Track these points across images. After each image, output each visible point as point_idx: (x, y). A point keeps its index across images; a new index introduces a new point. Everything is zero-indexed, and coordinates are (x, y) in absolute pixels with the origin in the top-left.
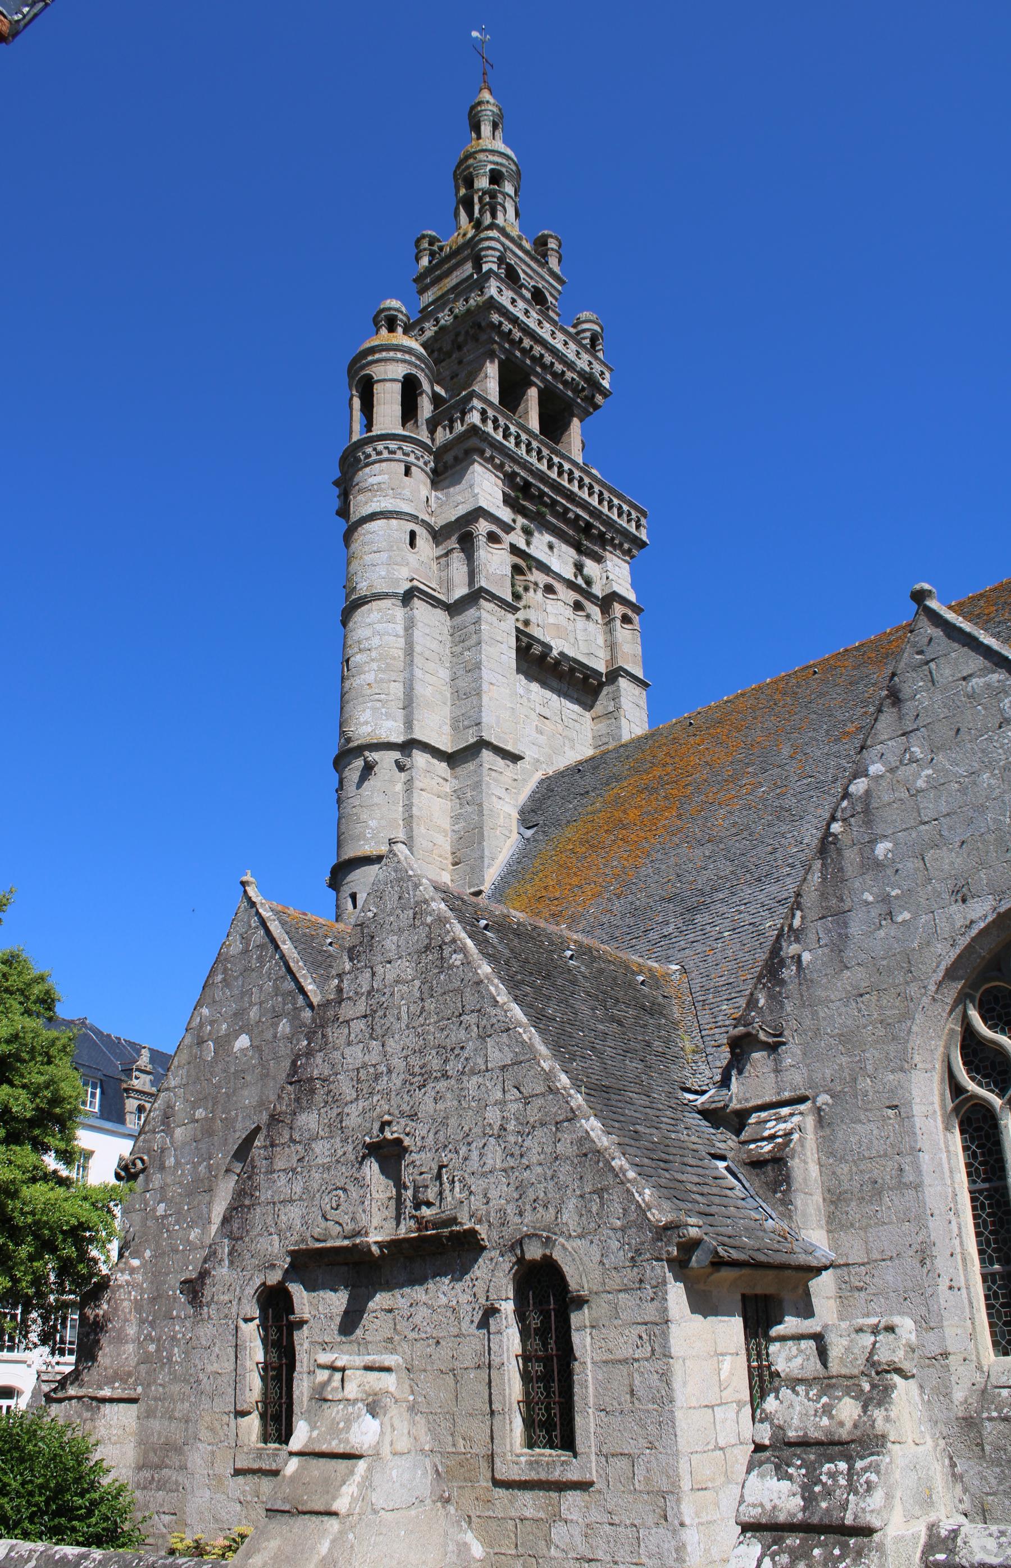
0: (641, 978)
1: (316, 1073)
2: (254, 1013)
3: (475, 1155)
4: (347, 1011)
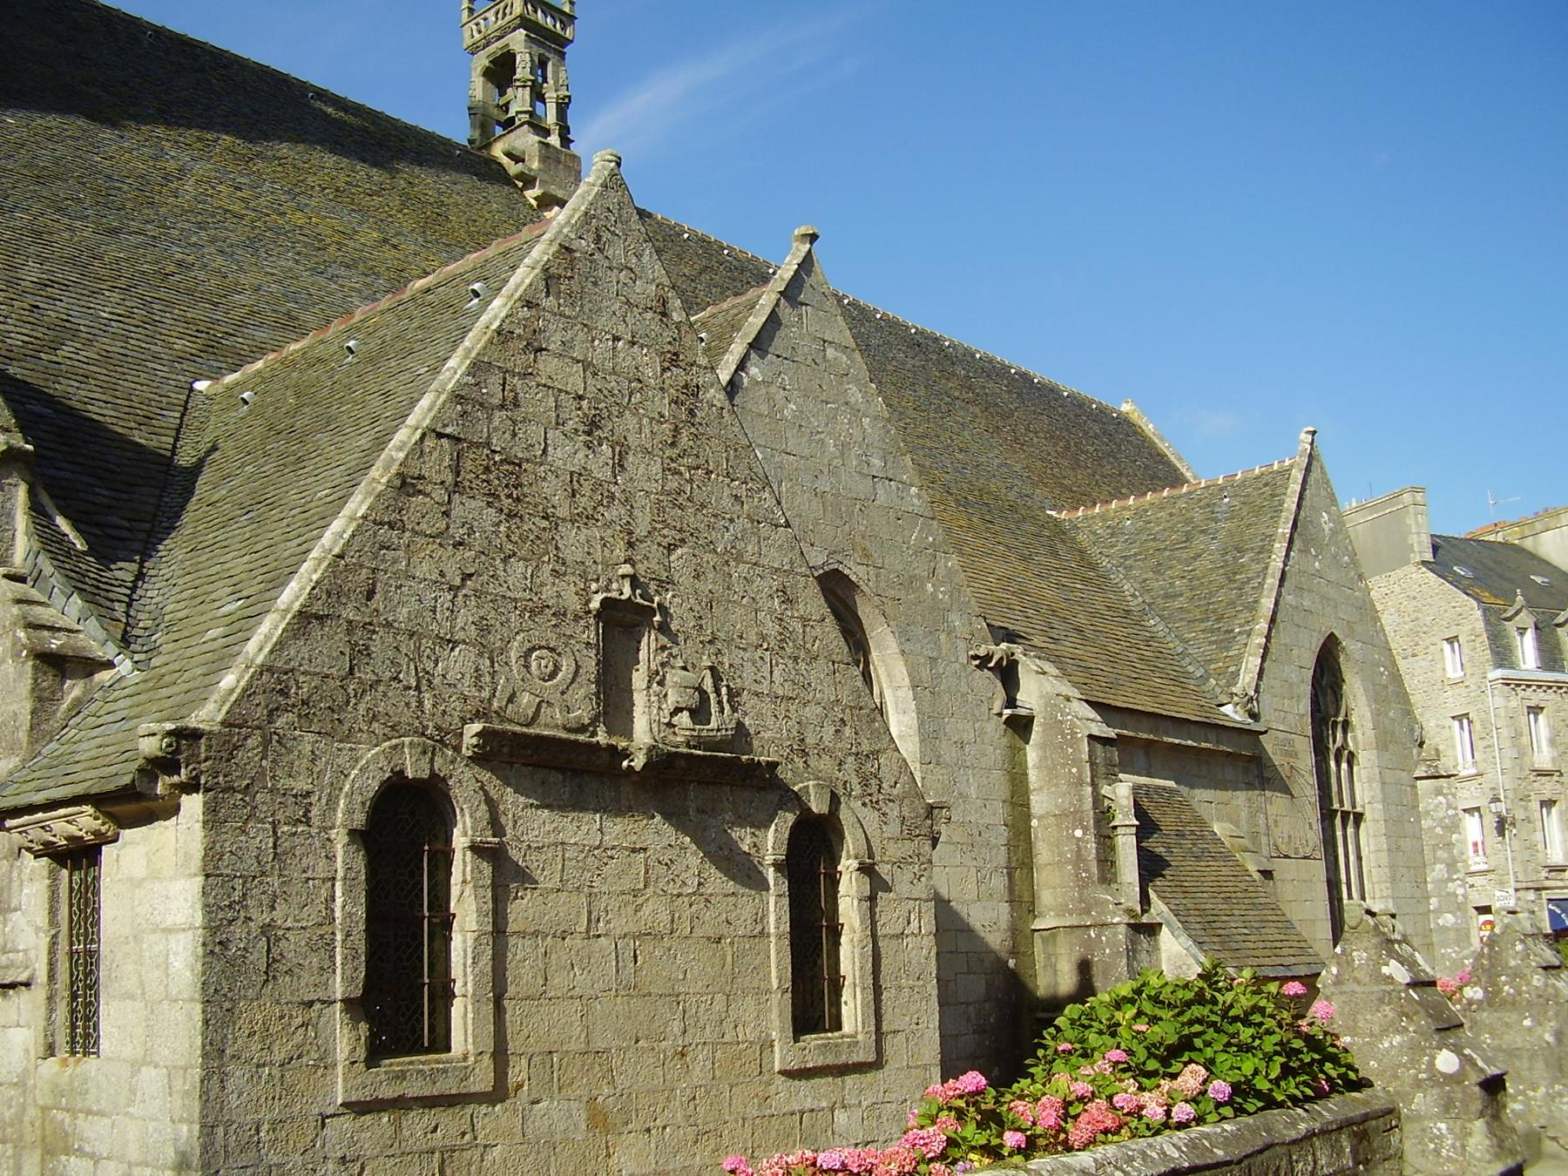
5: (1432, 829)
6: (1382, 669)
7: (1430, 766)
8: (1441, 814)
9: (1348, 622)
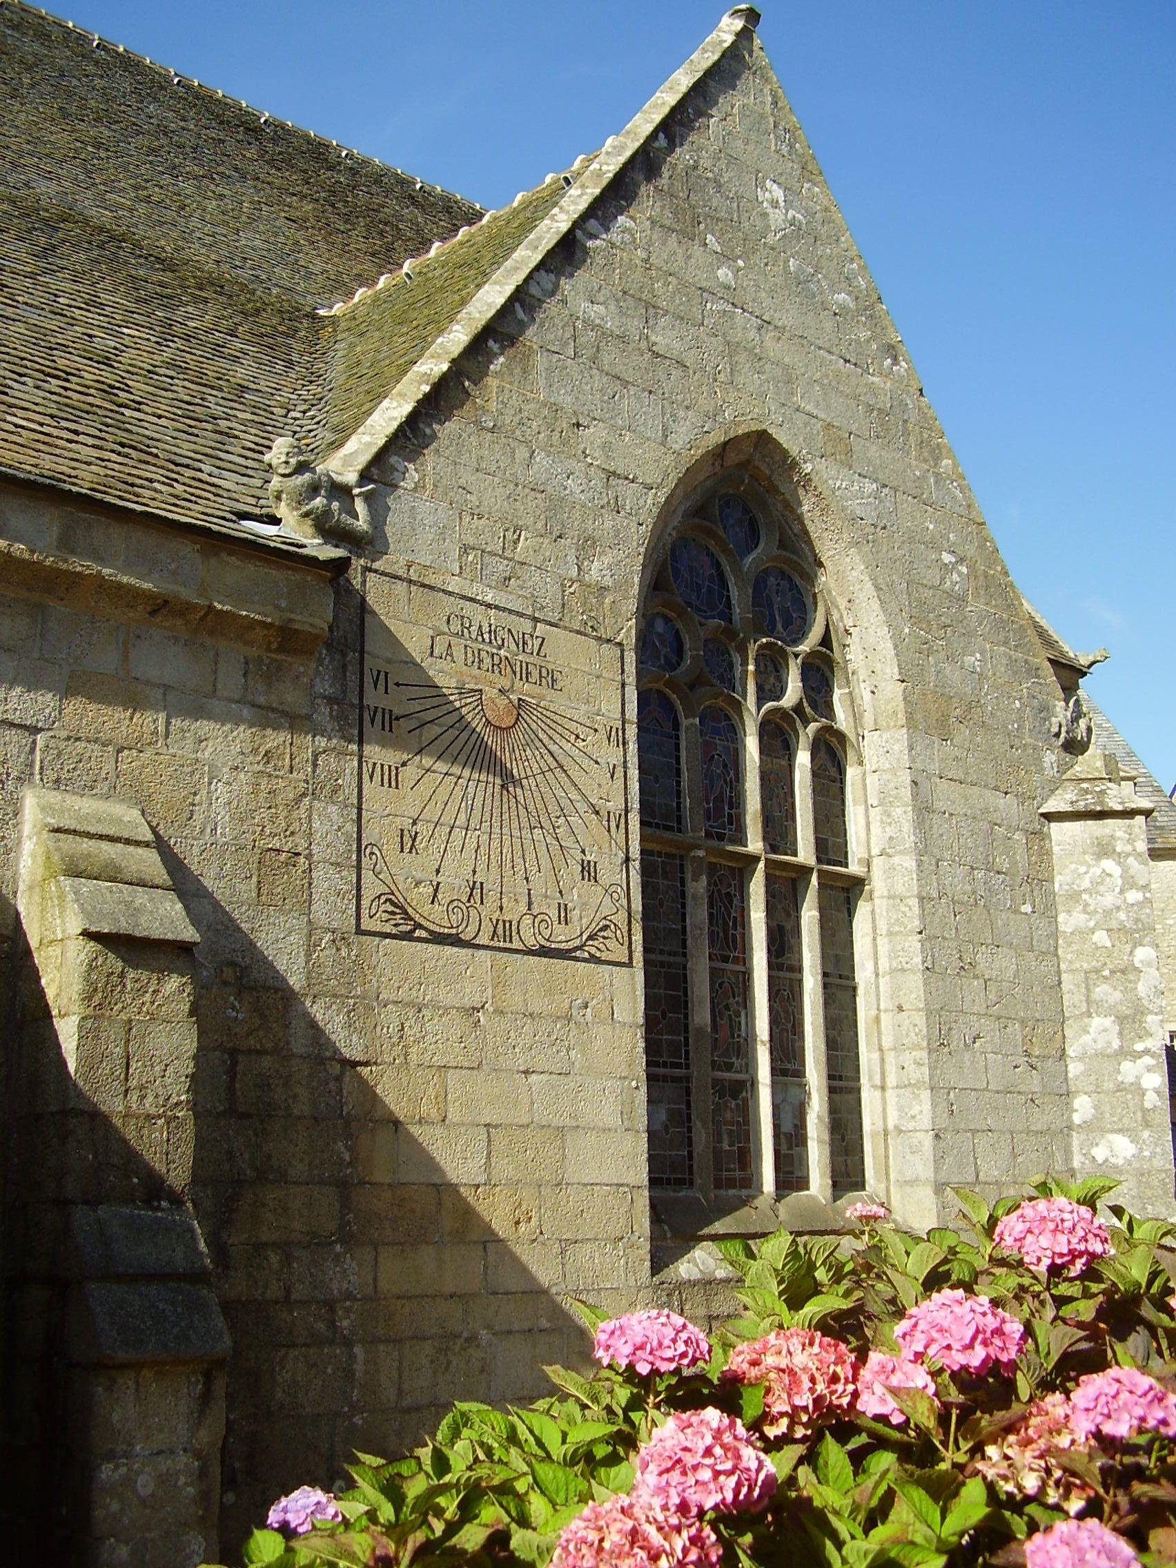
5: (1083, 934)
6: (947, 558)
7: (1086, 791)
8: (1109, 900)
9: (829, 426)
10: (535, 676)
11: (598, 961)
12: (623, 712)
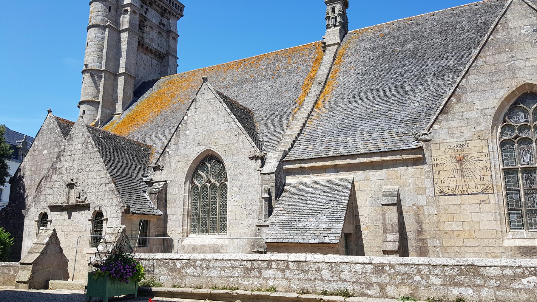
0: (142, 149)
1: (58, 167)
2: (49, 145)
3: (89, 188)
4: (66, 154)
10: (467, 150)
11: (485, 194)
12: (489, 150)
